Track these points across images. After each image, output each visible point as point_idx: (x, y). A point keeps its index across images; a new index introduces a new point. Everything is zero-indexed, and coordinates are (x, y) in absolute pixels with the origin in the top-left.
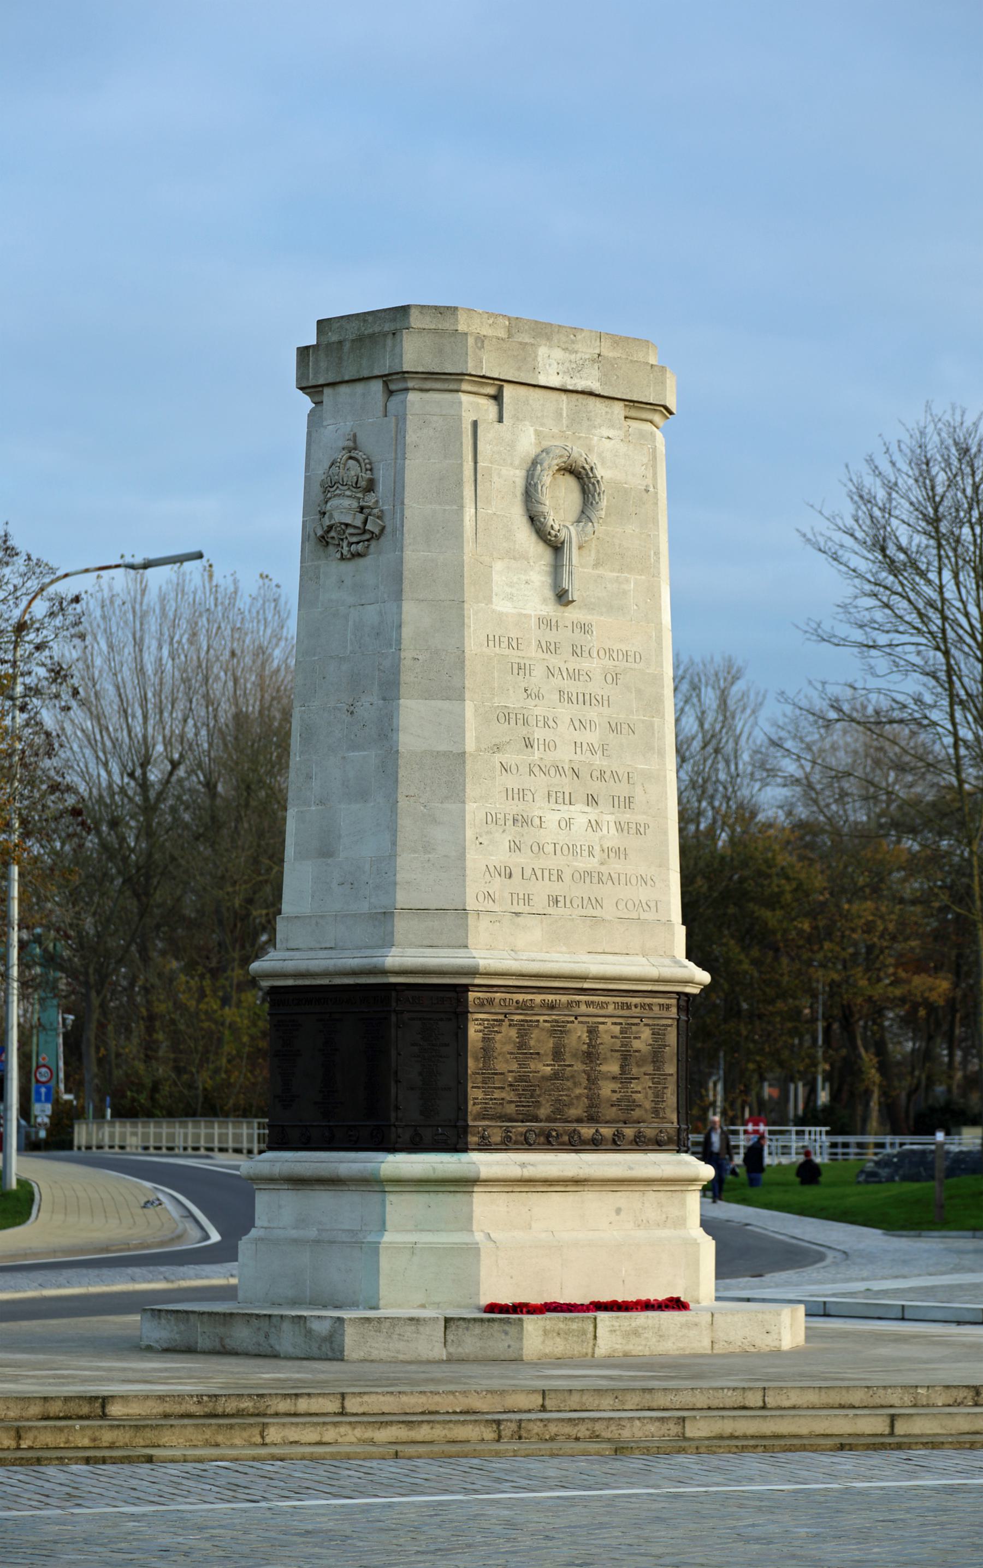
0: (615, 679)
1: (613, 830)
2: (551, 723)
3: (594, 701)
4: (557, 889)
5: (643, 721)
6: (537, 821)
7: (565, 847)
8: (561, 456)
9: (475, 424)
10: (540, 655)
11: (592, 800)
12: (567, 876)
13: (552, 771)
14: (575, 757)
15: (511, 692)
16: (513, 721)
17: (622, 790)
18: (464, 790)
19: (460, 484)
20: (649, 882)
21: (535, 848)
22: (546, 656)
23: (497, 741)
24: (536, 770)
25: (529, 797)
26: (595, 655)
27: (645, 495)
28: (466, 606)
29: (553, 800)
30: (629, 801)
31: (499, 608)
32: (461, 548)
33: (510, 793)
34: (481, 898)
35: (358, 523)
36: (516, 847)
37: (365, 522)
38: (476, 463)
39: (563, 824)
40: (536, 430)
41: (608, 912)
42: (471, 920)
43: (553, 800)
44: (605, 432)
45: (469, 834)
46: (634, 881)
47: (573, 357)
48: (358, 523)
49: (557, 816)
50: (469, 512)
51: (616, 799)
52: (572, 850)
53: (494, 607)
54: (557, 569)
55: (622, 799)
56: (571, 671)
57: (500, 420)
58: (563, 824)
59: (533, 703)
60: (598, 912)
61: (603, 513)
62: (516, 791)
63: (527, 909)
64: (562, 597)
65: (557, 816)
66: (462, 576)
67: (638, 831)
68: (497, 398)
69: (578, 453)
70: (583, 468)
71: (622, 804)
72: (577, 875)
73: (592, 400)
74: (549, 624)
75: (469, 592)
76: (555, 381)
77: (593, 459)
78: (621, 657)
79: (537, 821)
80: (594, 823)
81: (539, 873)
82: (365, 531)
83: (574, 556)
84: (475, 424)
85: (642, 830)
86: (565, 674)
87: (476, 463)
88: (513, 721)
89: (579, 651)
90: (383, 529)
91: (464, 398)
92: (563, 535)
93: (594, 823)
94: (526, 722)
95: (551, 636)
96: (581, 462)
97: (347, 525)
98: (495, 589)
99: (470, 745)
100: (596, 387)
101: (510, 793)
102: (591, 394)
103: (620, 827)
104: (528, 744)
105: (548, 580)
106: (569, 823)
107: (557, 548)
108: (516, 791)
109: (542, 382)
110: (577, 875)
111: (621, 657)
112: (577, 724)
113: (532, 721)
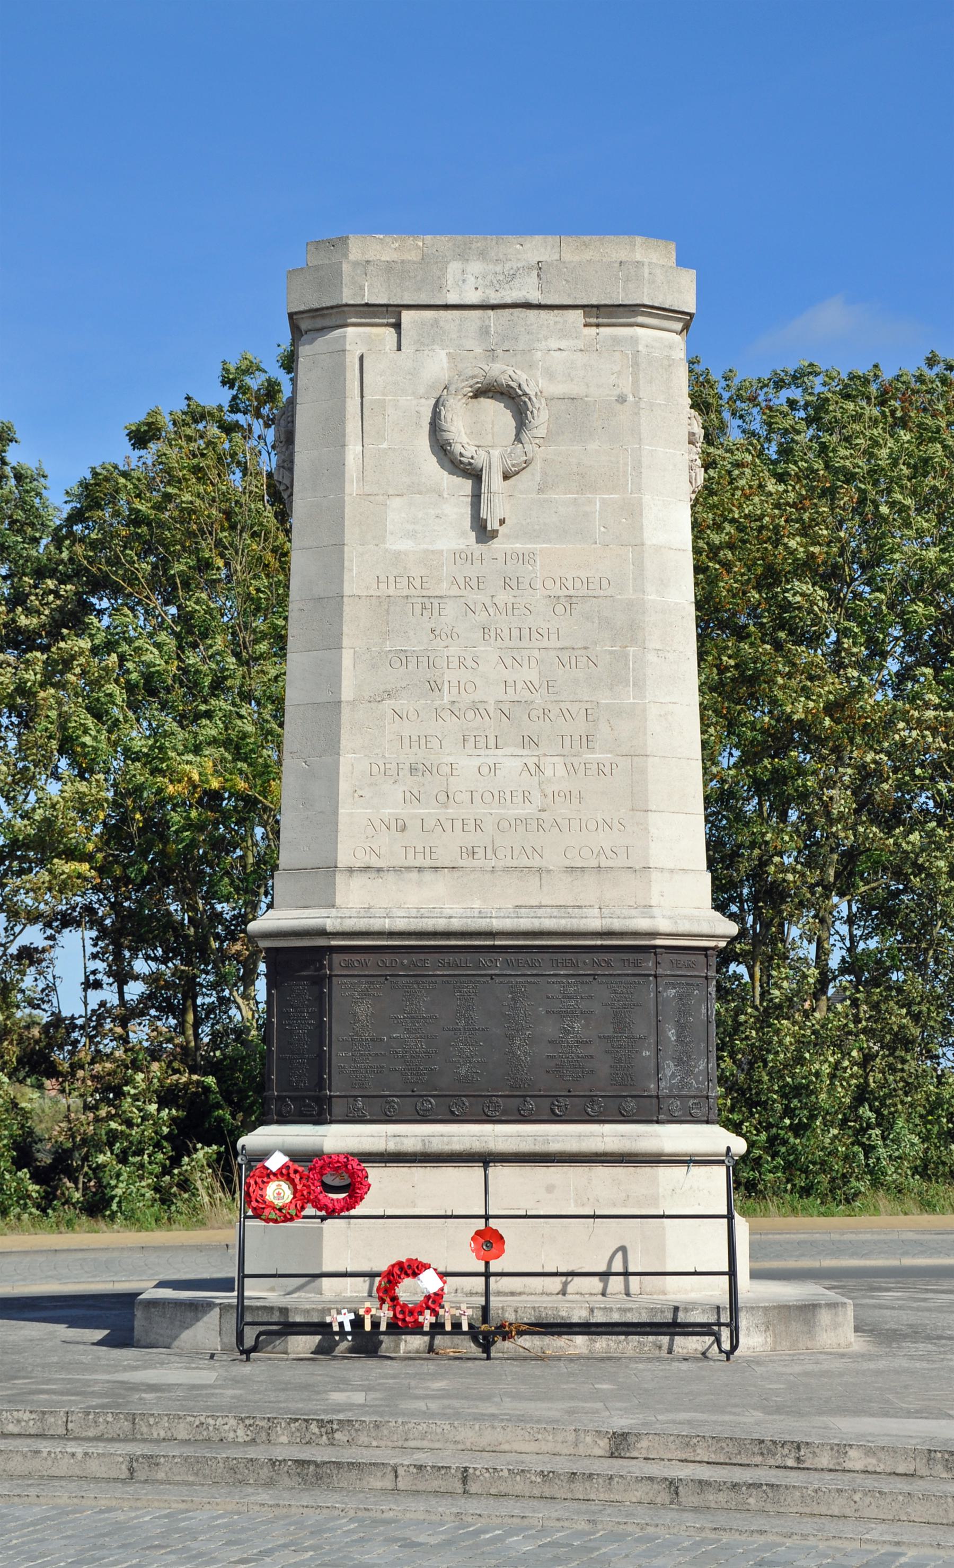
1: (561, 771)
2: (470, 663)
3: (535, 635)
4: (473, 839)
5: (611, 653)
6: (446, 769)
7: (487, 794)
8: (473, 377)
9: (361, 358)
11: (529, 741)
12: (488, 826)
14: (505, 698)
15: (411, 633)
18: (339, 742)
19: (342, 421)
20: (616, 825)
21: (442, 798)
23: (389, 687)
24: (446, 714)
25: (435, 743)
26: (539, 585)
27: (618, 406)
28: (346, 548)
31: (394, 547)
32: (342, 489)
33: (406, 741)
34: (360, 854)
38: (362, 397)
39: (485, 770)
40: (448, 354)
41: (553, 859)
42: (340, 879)
45: (344, 786)
46: (592, 826)
47: (499, 268)
49: (477, 762)
50: (353, 451)
53: (387, 546)
54: (476, 497)
57: (399, 349)
58: (485, 770)
60: (536, 862)
61: (541, 432)
62: (414, 738)
63: (428, 863)
65: (477, 762)
66: (343, 518)
68: (397, 326)
69: (501, 371)
70: (508, 386)
73: (532, 313)
74: (469, 559)
75: (351, 535)
76: (473, 297)
77: (522, 376)
78: (578, 584)
79: (446, 769)
80: (532, 768)
81: (448, 825)
83: (494, 482)
84: (361, 358)
85: (607, 770)
87: (362, 397)
89: (514, 584)
91: (350, 330)
92: (480, 460)
93: (532, 768)
94: (431, 665)
95: (472, 571)
96: (504, 379)
98: (390, 527)
99: (347, 692)
100: (535, 297)
101: (406, 741)
102: (528, 306)
105: (468, 511)
107: (475, 475)
108: (414, 738)
109: (452, 299)
111: (578, 584)
112: (509, 662)
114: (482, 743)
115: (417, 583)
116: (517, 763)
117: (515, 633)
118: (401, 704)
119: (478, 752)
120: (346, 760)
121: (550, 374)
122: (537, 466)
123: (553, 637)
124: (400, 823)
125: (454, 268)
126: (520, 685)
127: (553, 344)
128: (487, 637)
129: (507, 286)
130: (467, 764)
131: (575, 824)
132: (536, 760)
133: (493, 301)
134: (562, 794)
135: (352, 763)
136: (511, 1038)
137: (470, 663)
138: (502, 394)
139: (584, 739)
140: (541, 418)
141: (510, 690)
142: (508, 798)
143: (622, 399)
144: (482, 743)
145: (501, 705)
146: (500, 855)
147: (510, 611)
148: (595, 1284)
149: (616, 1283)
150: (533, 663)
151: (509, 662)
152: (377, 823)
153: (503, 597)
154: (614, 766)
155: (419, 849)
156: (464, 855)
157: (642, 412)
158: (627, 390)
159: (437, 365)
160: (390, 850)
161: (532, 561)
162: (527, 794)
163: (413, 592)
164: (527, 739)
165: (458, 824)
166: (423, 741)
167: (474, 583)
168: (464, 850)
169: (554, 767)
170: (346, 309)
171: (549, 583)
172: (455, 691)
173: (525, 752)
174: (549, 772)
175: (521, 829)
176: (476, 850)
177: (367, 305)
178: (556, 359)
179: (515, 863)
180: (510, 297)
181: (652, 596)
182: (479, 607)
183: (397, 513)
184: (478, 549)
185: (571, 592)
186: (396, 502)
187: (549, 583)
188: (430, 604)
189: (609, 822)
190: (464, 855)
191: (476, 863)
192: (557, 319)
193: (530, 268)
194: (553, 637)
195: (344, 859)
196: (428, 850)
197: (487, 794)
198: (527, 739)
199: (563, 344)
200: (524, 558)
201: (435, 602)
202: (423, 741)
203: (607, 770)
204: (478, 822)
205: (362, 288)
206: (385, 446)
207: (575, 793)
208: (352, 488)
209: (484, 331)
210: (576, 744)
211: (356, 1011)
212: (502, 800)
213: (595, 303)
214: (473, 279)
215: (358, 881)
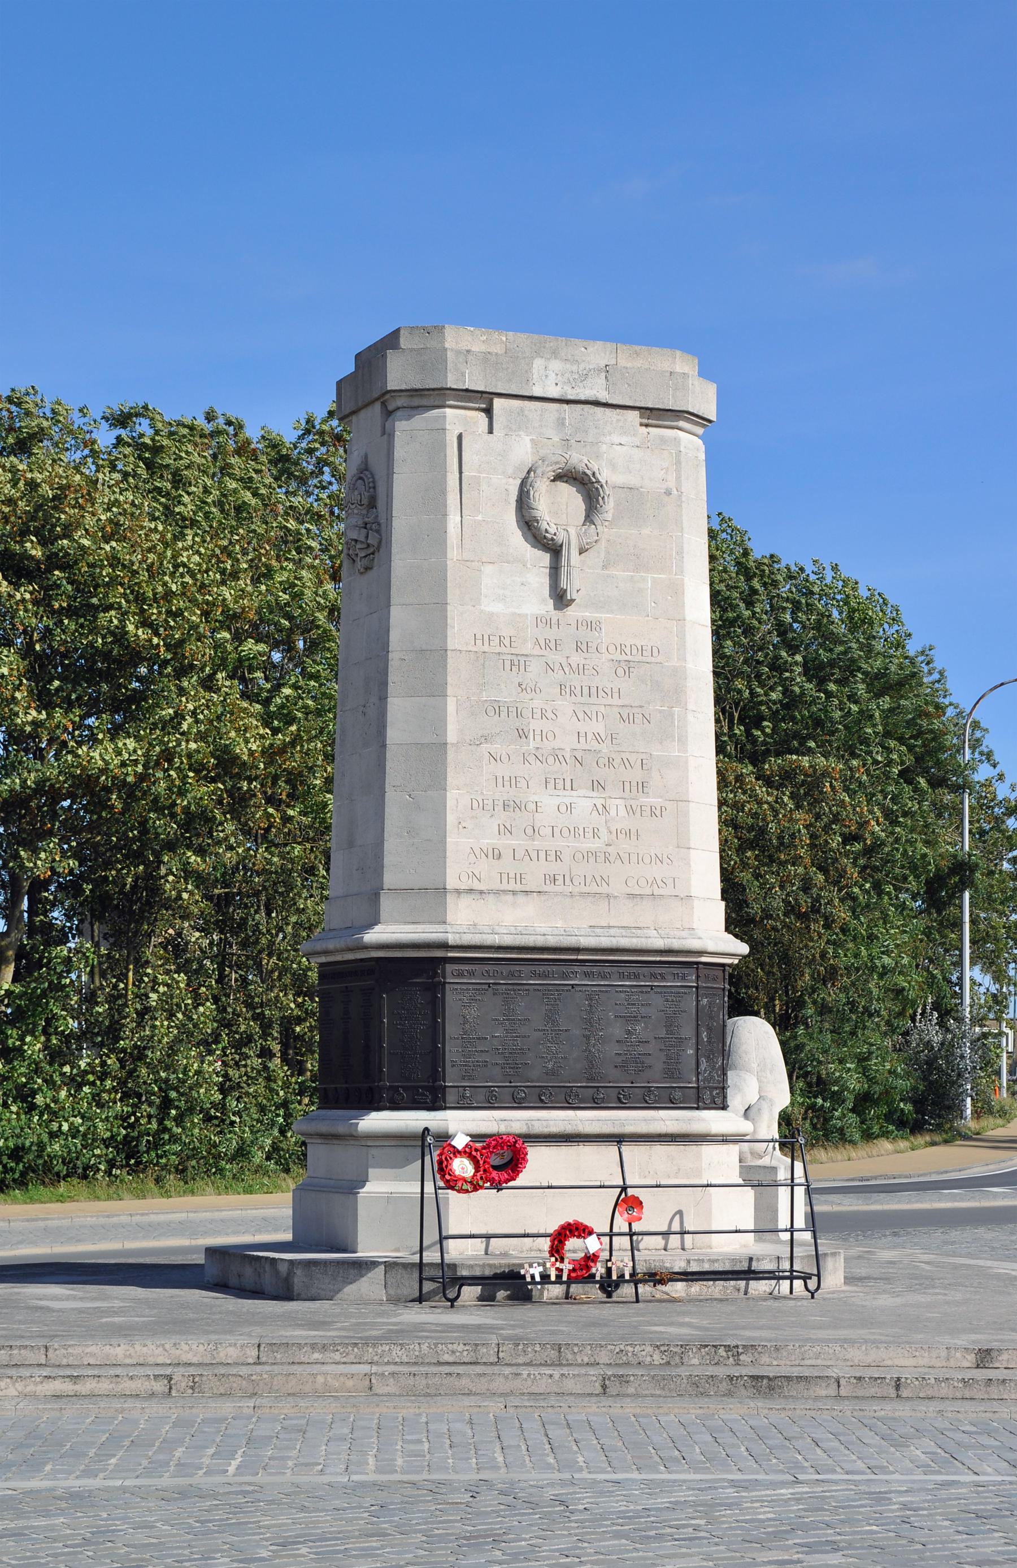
0: (628, 672)
1: (622, 812)
2: (550, 715)
4: (554, 868)
5: (660, 712)
6: (531, 807)
7: (565, 830)
8: (557, 463)
9: (460, 437)
10: (537, 651)
11: (597, 785)
12: (566, 856)
13: (551, 760)
14: (578, 746)
15: (503, 686)
16: (504, 714)
17: (636, 775)
18: (445, 779)
19: (443, 492)
20: (666, 860)
21: (529, 831)
22: (543, 652)
23: (486, 733)
24: (531, 759)
25: (523, 784)
26: (604, 650)
27: (666, 499)
28: (449, 607)
29: (551, 786)
30: (643, 786)
31: (487, 609)
32: (444, 554)
33: (500, 780)
34: (464, 878)
35: (362, 538)
36: (506, 830)
37: (367, 537)
38: (461, 473)
39: (563, 809)
40: (532, 440)
41: (616, 888)
42: (450, 899)
43: (551, 786)
44: (616, 439)
45: (451, 818)
46: (647, 860)
47: (574, 368)
48: (362, 538)
49: (557, 801)
50: (453, 520)
51: (627, 785)
52: (574, 832)
53: (482, 607)
54: (555, 570)
55: (634, 784)
56: (575, 666)
57: (491, 431)
58: (563, 809)
59: (529, 697)
60: (604, 889)
61: (609, 516)
62: (507, 778)
63: (518, 887)
64: (560, 598)
65: (557, 801)
66: (445, 580)
67: (652, 813)
68: (488, 411)
69: (579, 459)
70: (584, 473)
71: (634, 789)
72: (579, 856)
73: (599, 410)
74: (549, 623)
75: (453, 595)
76: (554, 392)
77: (594, 466)
78: (634, 651)
79: (531, 807)
82: (368, 546)
83: (572, 557)
84: (460, 437)
85: (658, 813)
86: (567, 669)
87: (461, 473)
88: (504, 714)
90: (380, 542)
91: (448, 410)
92: (561, 537)
94: (519, 714)
95: (552, 634)
96: (582, 467)
97: (356, 541)
98: (484, 591)
99: (452, 736)
100: (603, 396)
101: (500, 780)
102: (597, 403)
103: (631, 810)
104: (522, 734)
105: (546, 581)
106: (570, 807)
107: (555, 550)
108: (507, 778)
109: (537, 392)
110: (579, 856)
111: (634, 651)
112: (581, 715)
113: (527, 713)
114: (560, 786)
115: (507, 642)
116: (588, 804)
117: (586, 691)
118: (496, 748)
119: (557, 792)
120: (452, 796)
121: (613, 466)
122: (603, 543)
124: (496, 852)
125: (538, 363)
126: (590, 736)
127: (616, 439)
129: (581, 385)
130: (549, 801)
131: (634, 858)
132: (602, 801)
134: (623, 832)
135: (457, 798)
136: (587, 1038)
137: (550, 715)
138: (575, 479)
139: (640, 785)
140: (609, 506)
141: (582, 740)
142: (581, 832)
143: (668, 493)
144: (560, 786)
145: (576, 753)
146: (576, 883)
147: (581, 671)
148: (659, 1241)
149: (674, 1240)
150: (600, 718)
151: (581, 715)
152: (478, 852)
153: (576, 659)
156: (548, 882)
157: (683, 505)
158: (671, 484)
159: (522, 450)
160: (488, 873)
161: (598, 629)
163: (503, 649)
165: (542, 855)
167: (552, 645)
168: (547, 877)
169: (617, 807)
170: (448, 392)
171: (612, 648)
172: (538, 738)
173: (594, 794)
174: (613, 812)
175: (592, 860)
176: (557, 877)
178: (620, 452)
179: (586, 889)
181: (690, 665)
182: (557, 666)
183: (489, 577)
184: (555, 615)
185: (629, 658)
186: (488, 569)
187: (612, 648)
188: (517, 662)
189: (660, 856)
190: (548, 882)
191: (557, 889)
192: (619, 417)
193: (600, 370)
195: (451, 883)
196: (518, 876)
197: (565, 830)
200: (592, 625)
201: (522, 659)
203: (658, 813)
204: (558, 853)
205: (463, 375)
206: (480, 518)
207: (633, 831)
208: (453, 553)
209: (561, 423)
210: (634, 789)
211: (464, 1011)
213: (651, 406)
214: (554, 375)
215: (465, 901)
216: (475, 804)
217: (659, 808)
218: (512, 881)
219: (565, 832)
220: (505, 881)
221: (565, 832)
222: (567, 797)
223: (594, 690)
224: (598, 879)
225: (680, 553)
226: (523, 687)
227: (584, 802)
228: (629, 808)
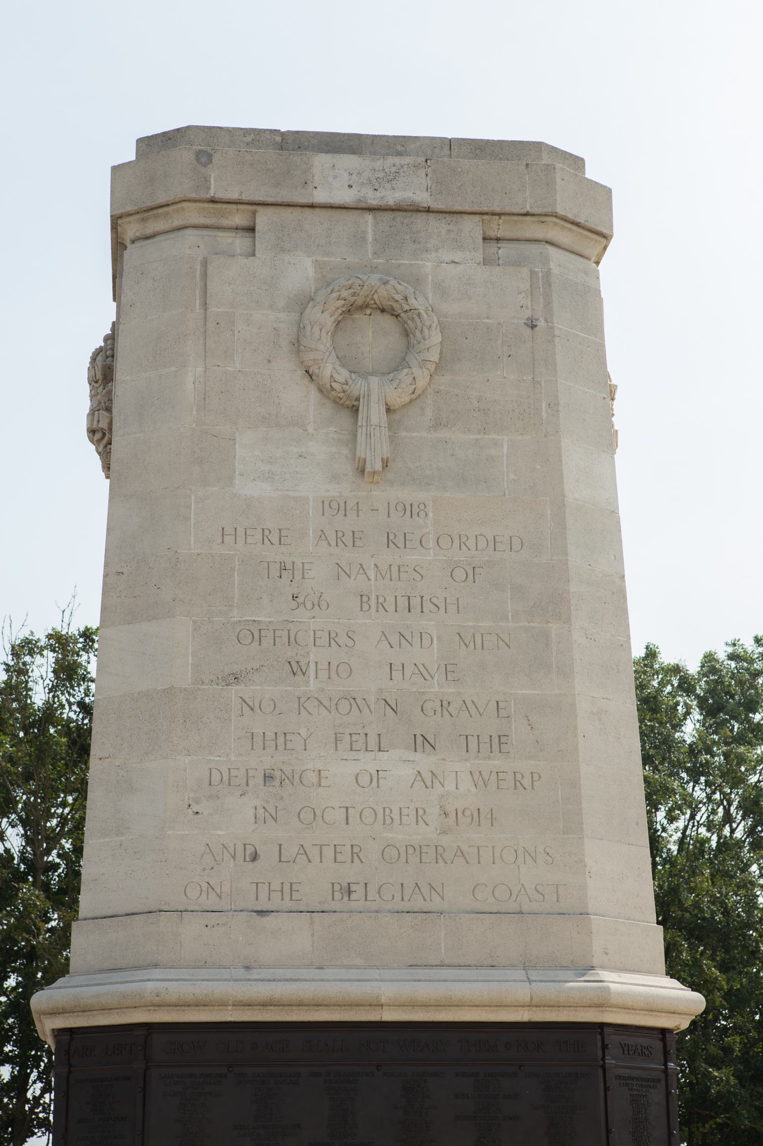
3: (428, 606)
6: (312, 777)
11: (423, 742)
16: (267, 642)
21: (307, 816)
26: (432, 544)
33: (258, 740)
39: (364, 780)
44: (446, 255)
58: (364, 780)
76: (345, 196)
78: (482, 544)
79: (312, 777)
81: (314, 853)
85: (526, 782)
86: (371, 574)
89: (400, 541)
100: (423, 198)
101: (258, 740)
104: (296, 670)
106: (377, 777)
109: (320, 196)
111: (482, 544)
114: (360, 745)
117: (402, 602)
119: (354, 755)
123: (452, 609)
128: (365, 607)
129: (388, 186)
133: (374, 203)
134: (468, 813)
138: (383, 311)
139: (495, 740)
141: (397, 675)
142: (396, 816)
146: (387, 896)
147: (395, 575)
154: (536, 777)
155: (276, 886)
156: (337, 895)
157: (557, 340)
162: (421, 812)
164: (420, 739)
165: (329, 853)
166: (281, 740)
167: (348, 539)
168: (337, 887)
170: (185, 204)
172: (323, 675)
173: (418, 756)
174: (450, 786)
175: (414, 859)
176: (353, 888)
177: (213, 201)
179: (406, 906)
180: (391, 197)
190: (337, 895)
191: (353, 905)
192: (450, 227)
194: (452, 609)
196: (287, 888)
197: (367, 812)
198: (420, 739)
199: (458, 256)
202: (281, 740)
203: (526, 782)
205: (207, 180)
210: (485, 747)
212: (388, 821)
214: (346, 175)
216: (216, 777)
217: (527, 776)
218: (276, 896)
219: (368, 816)
220: (263, 896)
221: (368, 816)
222: (368, 762)
223: (415, 602)
224: (425, 890)
225: (554, 406)
226: (300, 600)
227: (399, 767)
228: (476, 776)
